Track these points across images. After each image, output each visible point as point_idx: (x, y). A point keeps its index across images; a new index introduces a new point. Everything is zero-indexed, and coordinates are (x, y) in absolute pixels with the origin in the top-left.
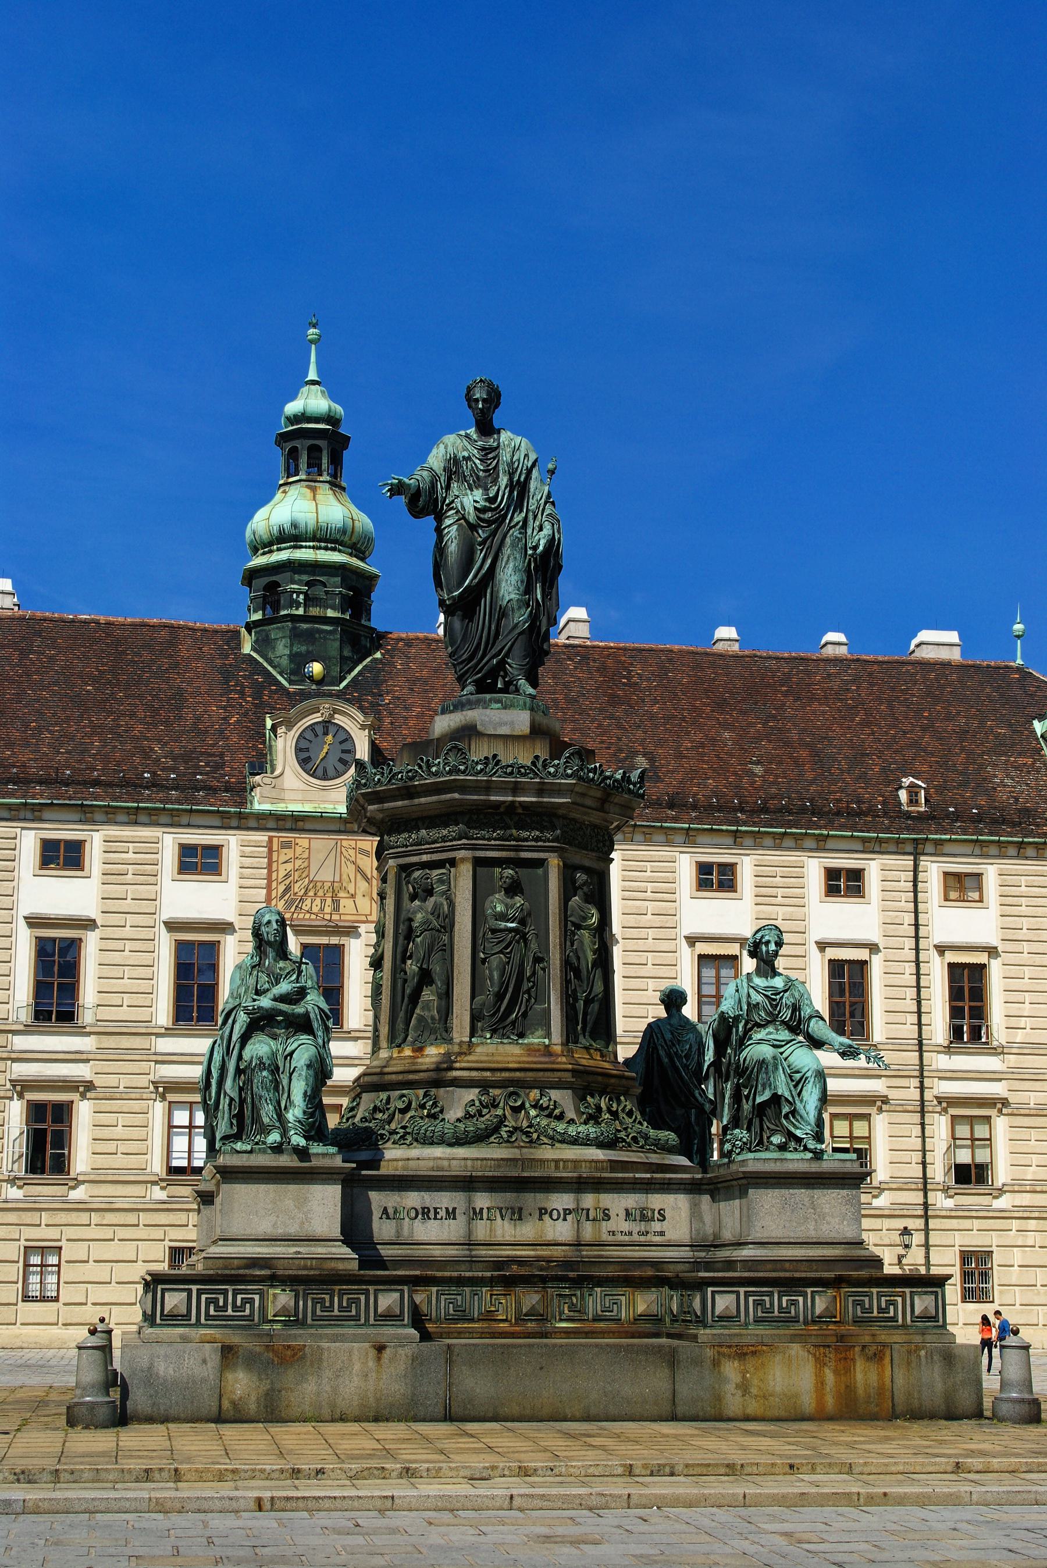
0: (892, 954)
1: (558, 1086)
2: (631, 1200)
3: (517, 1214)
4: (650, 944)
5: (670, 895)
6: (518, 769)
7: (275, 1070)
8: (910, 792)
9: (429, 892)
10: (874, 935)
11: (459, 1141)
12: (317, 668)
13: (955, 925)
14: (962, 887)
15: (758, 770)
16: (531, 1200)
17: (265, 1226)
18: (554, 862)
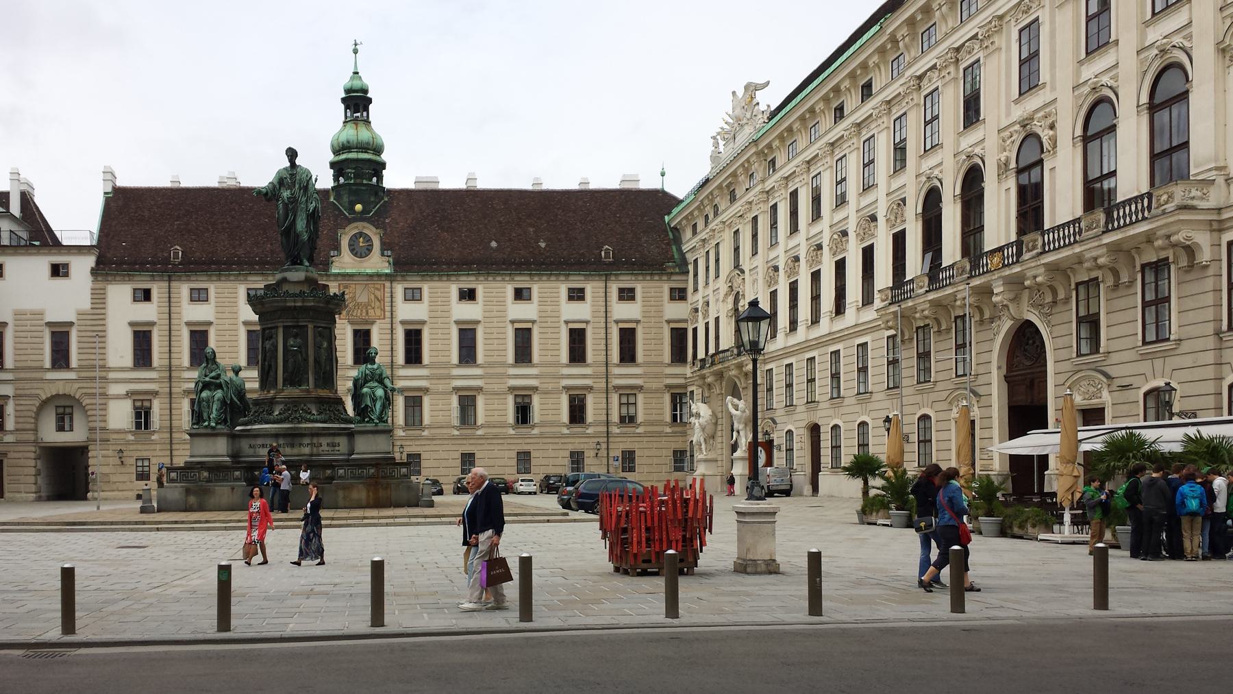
0: (596, 325)
1: (311, 402)
2: (329, 440)
3: (292, 446)
4: (495, 324)
5: (503, 303)
6: (295, 295)
7: (208, 402)
8: (607, 252)
9: (271, 337)
10: (587, 317)
11: (274, 422)
12: (359, 207)
13: (624, 311)
14: (627, 295)
15: (543, 245)
16: (297, 440)
17: (203, 452)
18: (310, 326)
